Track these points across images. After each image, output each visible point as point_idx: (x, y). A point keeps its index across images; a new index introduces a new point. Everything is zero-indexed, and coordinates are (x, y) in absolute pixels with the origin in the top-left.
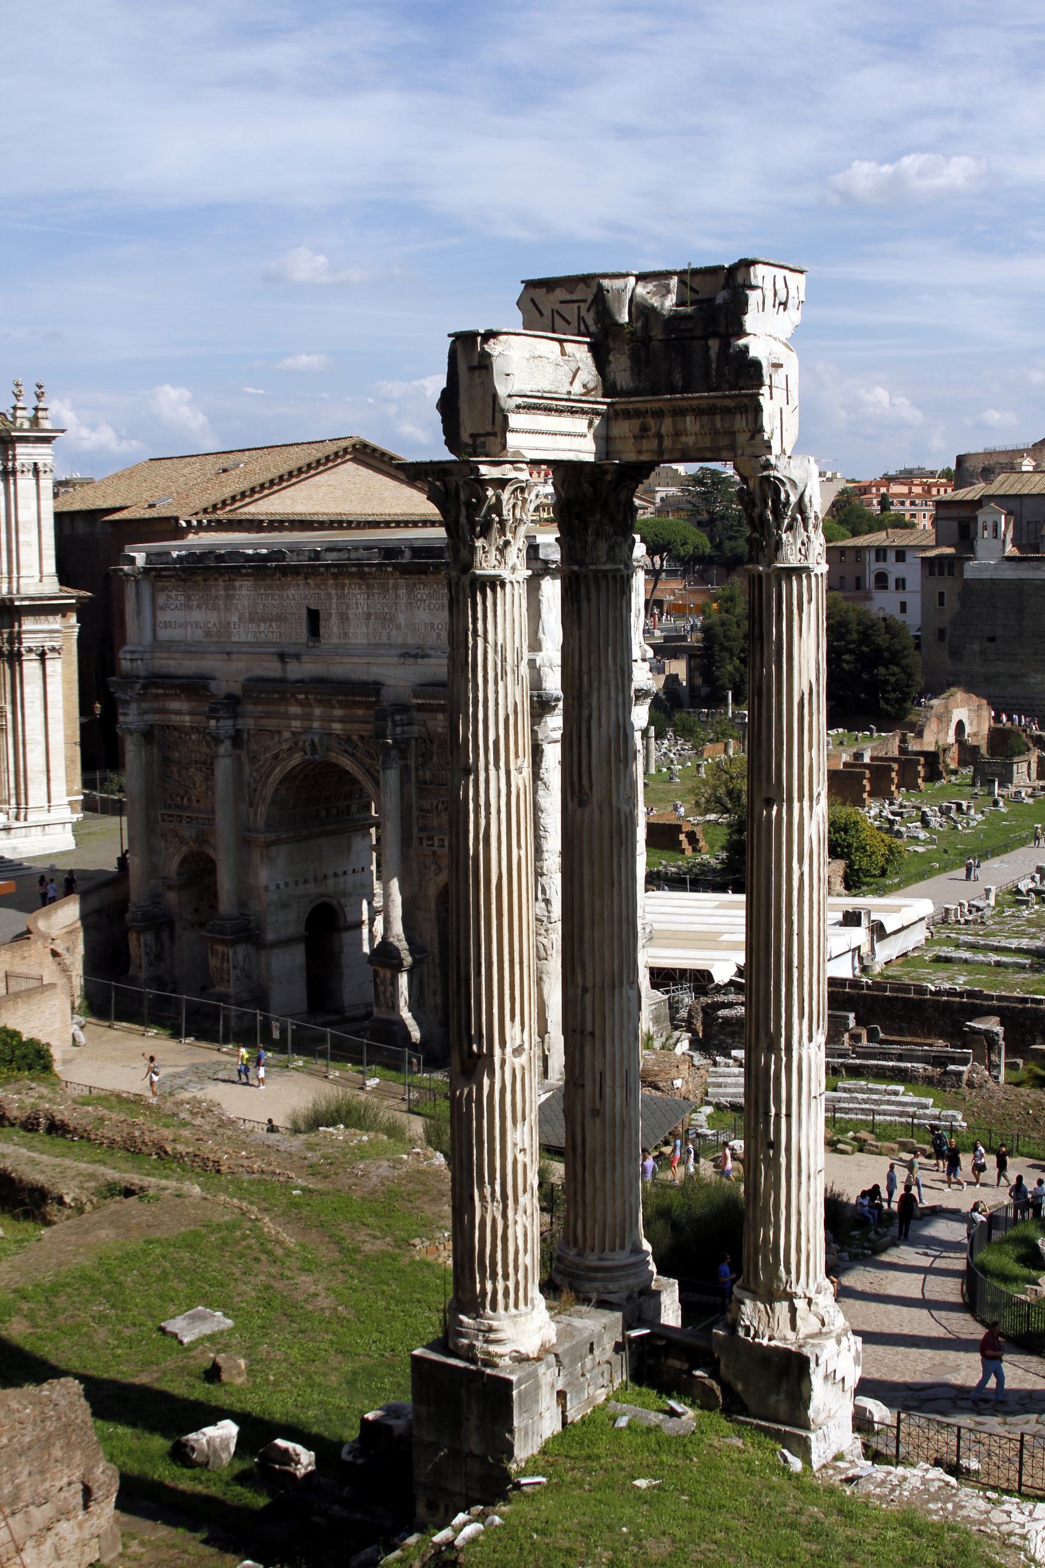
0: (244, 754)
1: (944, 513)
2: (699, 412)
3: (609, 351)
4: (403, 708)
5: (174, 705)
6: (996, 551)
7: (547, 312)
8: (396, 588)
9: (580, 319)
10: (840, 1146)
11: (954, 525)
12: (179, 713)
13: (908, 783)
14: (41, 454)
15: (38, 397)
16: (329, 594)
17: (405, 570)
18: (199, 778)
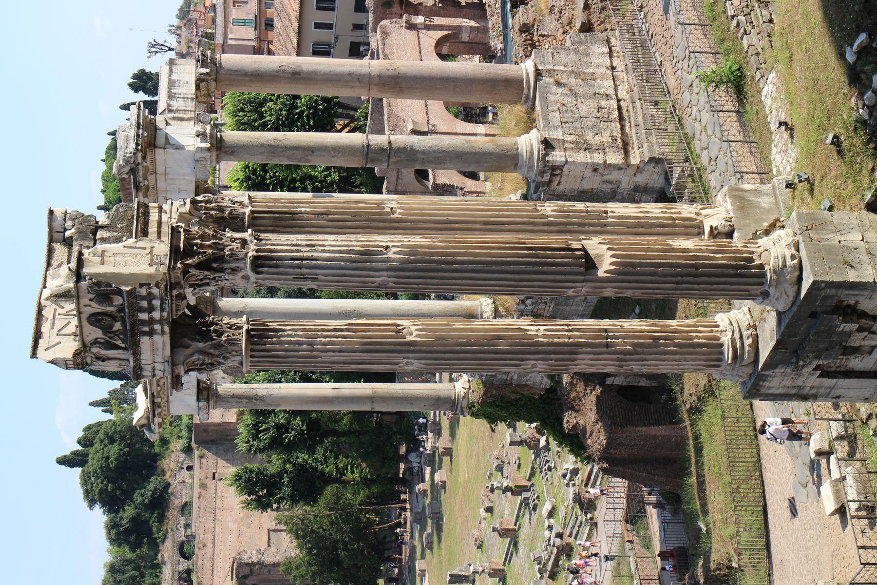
7: (59, 339)
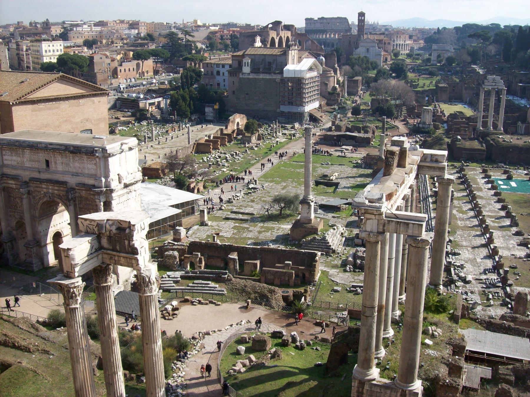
0: (31, 196)
1: (234, 58)
2: (124, 257)
3: (101, 237)
5: (10, 182)
8: (69, 157)
9: (93, 229)
10: (194, 303)
11: (237, 62)
12: (12, 184)
13: (223, 145)
16: (51, 157)
17: (72, 152)
18: (19, 201)
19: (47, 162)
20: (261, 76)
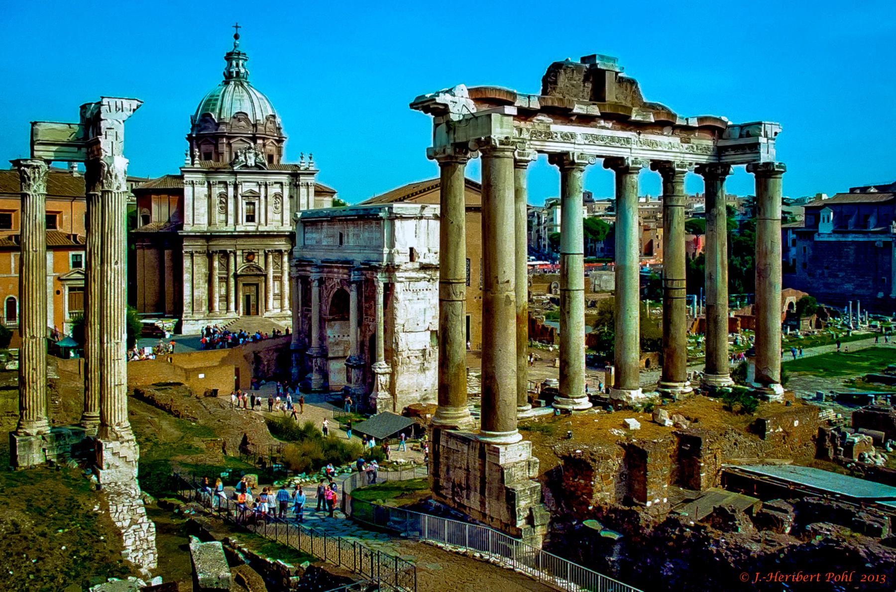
4: (358, 269)
6: (826, 229)
14: (311, 180)
15: (311, 158)
19: (341, 235)
20: (850, 238)
